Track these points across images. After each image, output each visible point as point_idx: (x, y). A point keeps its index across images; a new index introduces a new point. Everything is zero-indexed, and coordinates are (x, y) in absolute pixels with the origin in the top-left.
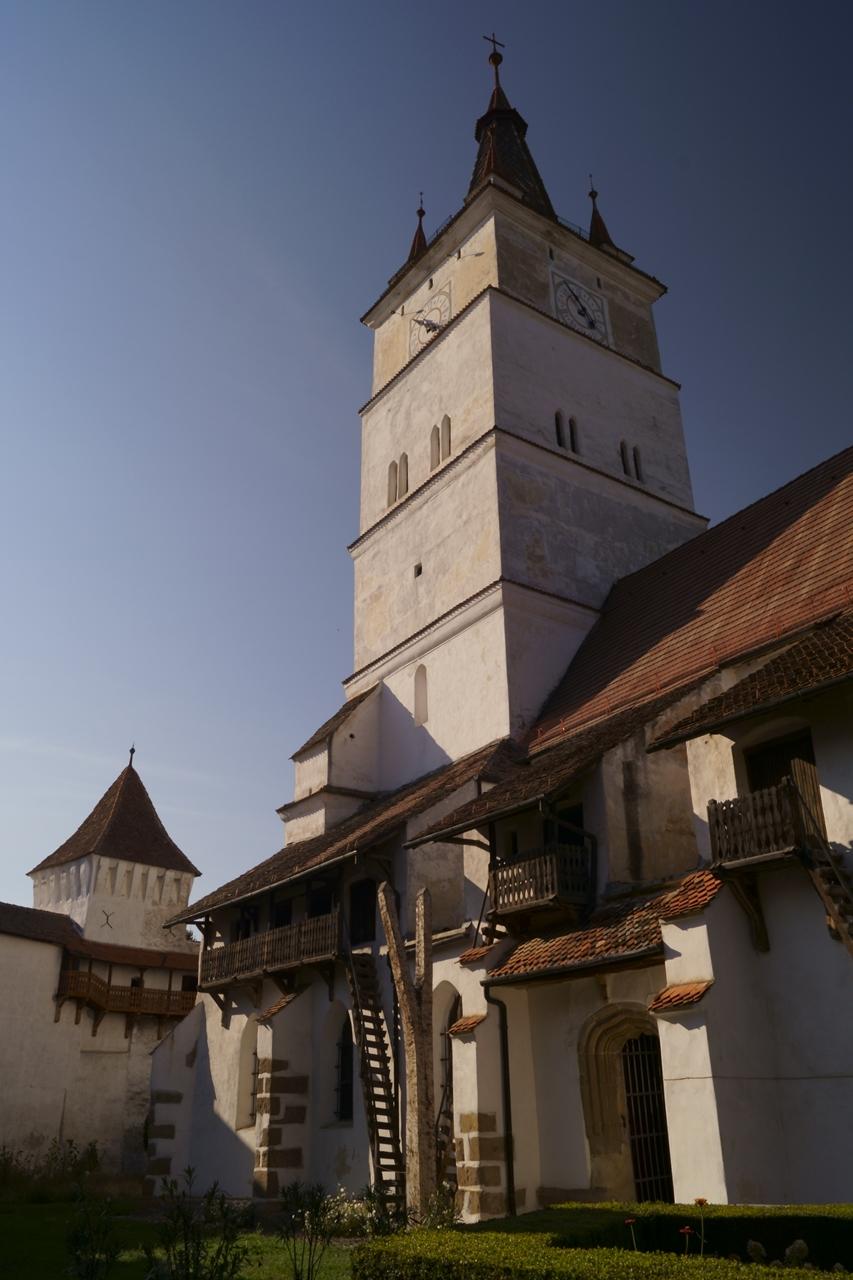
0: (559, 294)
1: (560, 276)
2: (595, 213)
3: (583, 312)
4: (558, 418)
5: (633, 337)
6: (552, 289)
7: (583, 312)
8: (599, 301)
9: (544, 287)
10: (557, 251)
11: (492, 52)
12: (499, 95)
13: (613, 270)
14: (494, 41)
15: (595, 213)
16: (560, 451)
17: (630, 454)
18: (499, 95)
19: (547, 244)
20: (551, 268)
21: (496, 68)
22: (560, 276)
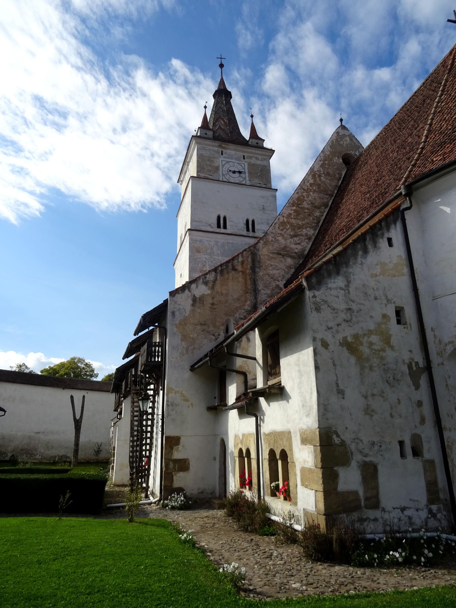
0: (224, 169)
1: (225, 161)
2: (252, 124)
3: (234, 172)
4: (219, 218)
5: (259, 174)
6: (221, 167)
7: (234, 172)
8: (243, 165)
9: (217, 168)
10: (224, 151)
11: (220, 63)
13: (250, 150)
14: (221, 58)
15: (252, 124)
16: (218, 230)
17: (250, 223)
19: (220, 150)
20: (221, 159)
21: (222, 70)
22: (225, 161)
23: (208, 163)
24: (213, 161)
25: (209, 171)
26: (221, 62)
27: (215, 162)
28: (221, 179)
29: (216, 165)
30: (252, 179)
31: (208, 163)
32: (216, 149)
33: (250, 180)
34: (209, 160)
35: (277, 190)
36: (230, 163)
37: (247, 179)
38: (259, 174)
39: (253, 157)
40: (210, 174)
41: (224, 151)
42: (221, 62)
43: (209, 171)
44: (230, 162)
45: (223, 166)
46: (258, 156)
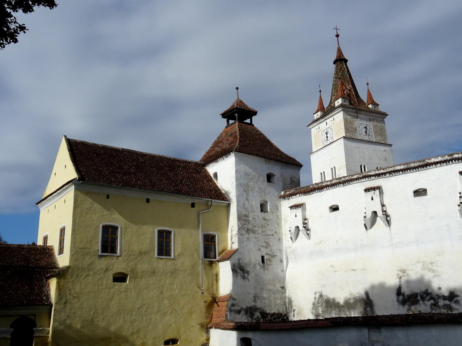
2: (368, 90)
5: (379, 133)
6: (358, 129)
8: (370, 126)
12: (339, 51)
14: (336, 29)
15: (368, 90)
18: (339, 51)
19: (356, 114)
23: (350, 125)
24: (353, 124)
25: (352, 131)
26: (337, 33)
27: (354, 124)
28: (359, 138)
29: (355, 127)
30: (376, 137)
31: (350, 125)
32: (353, 114)
33: (375, 137)
34: (350, 123)
35: (392, 145)
36: (362, 125)
37: (373, 136)
38: (379, 133)
39: (375, 119)
40: (352, 133)
41: (358, 115)
42: (337, 33)
43: (352, 131)
44: (363, 124)
45: (359, 127)
46: (378, 118)
